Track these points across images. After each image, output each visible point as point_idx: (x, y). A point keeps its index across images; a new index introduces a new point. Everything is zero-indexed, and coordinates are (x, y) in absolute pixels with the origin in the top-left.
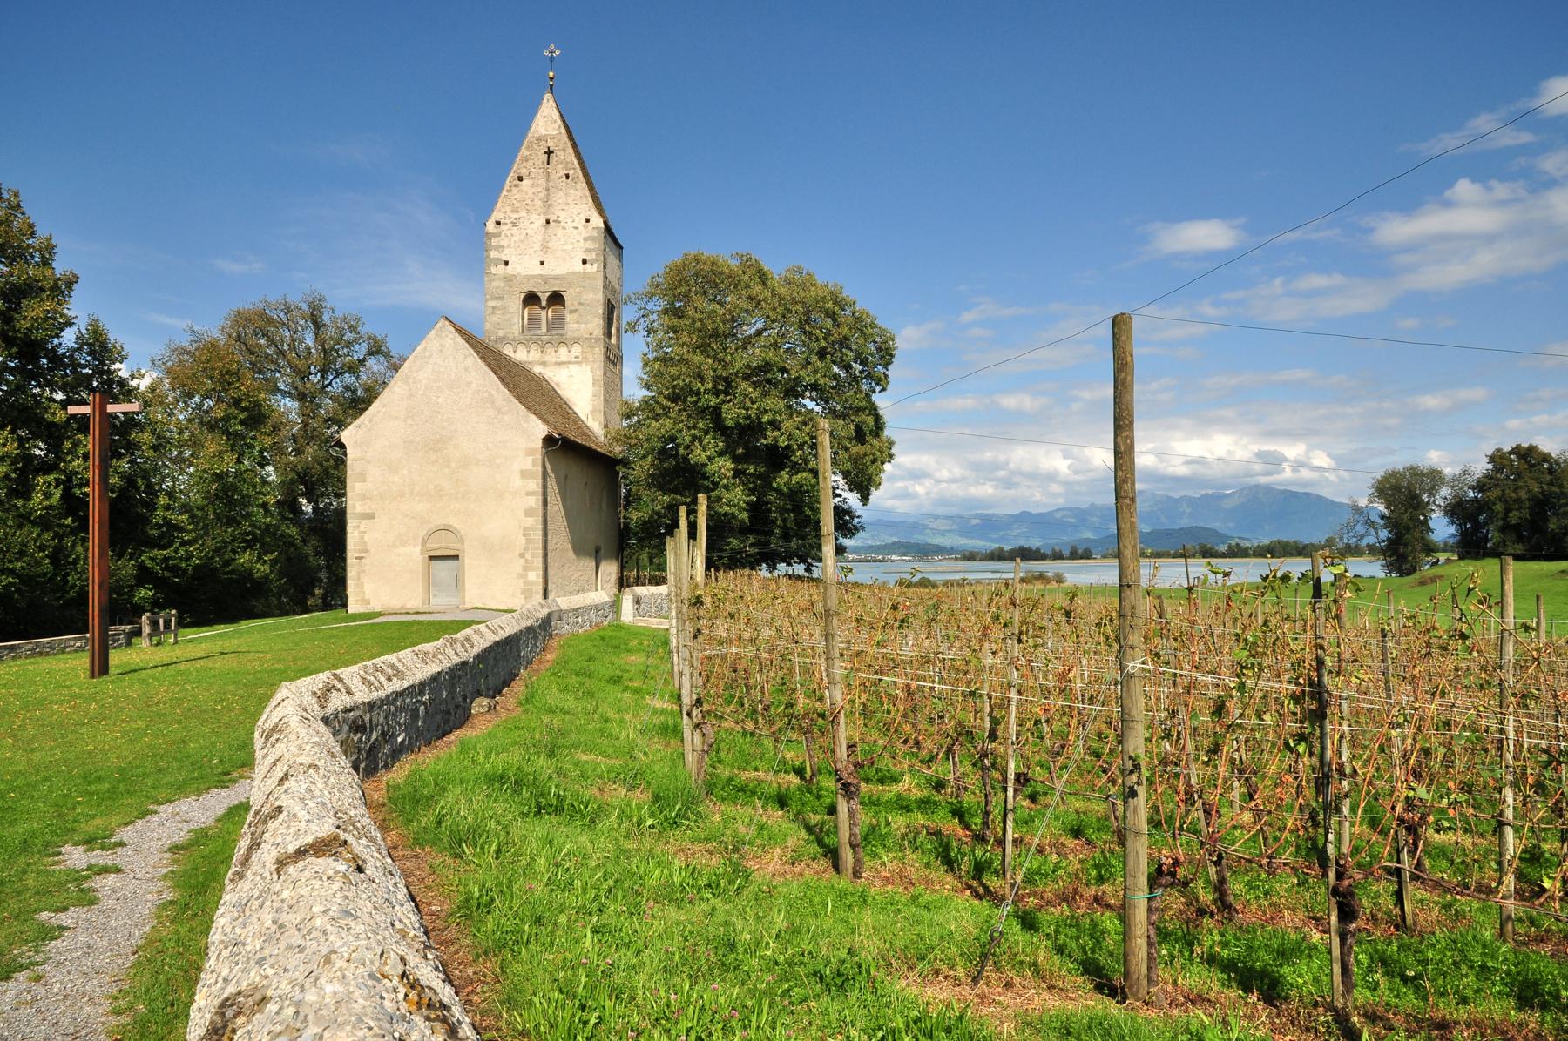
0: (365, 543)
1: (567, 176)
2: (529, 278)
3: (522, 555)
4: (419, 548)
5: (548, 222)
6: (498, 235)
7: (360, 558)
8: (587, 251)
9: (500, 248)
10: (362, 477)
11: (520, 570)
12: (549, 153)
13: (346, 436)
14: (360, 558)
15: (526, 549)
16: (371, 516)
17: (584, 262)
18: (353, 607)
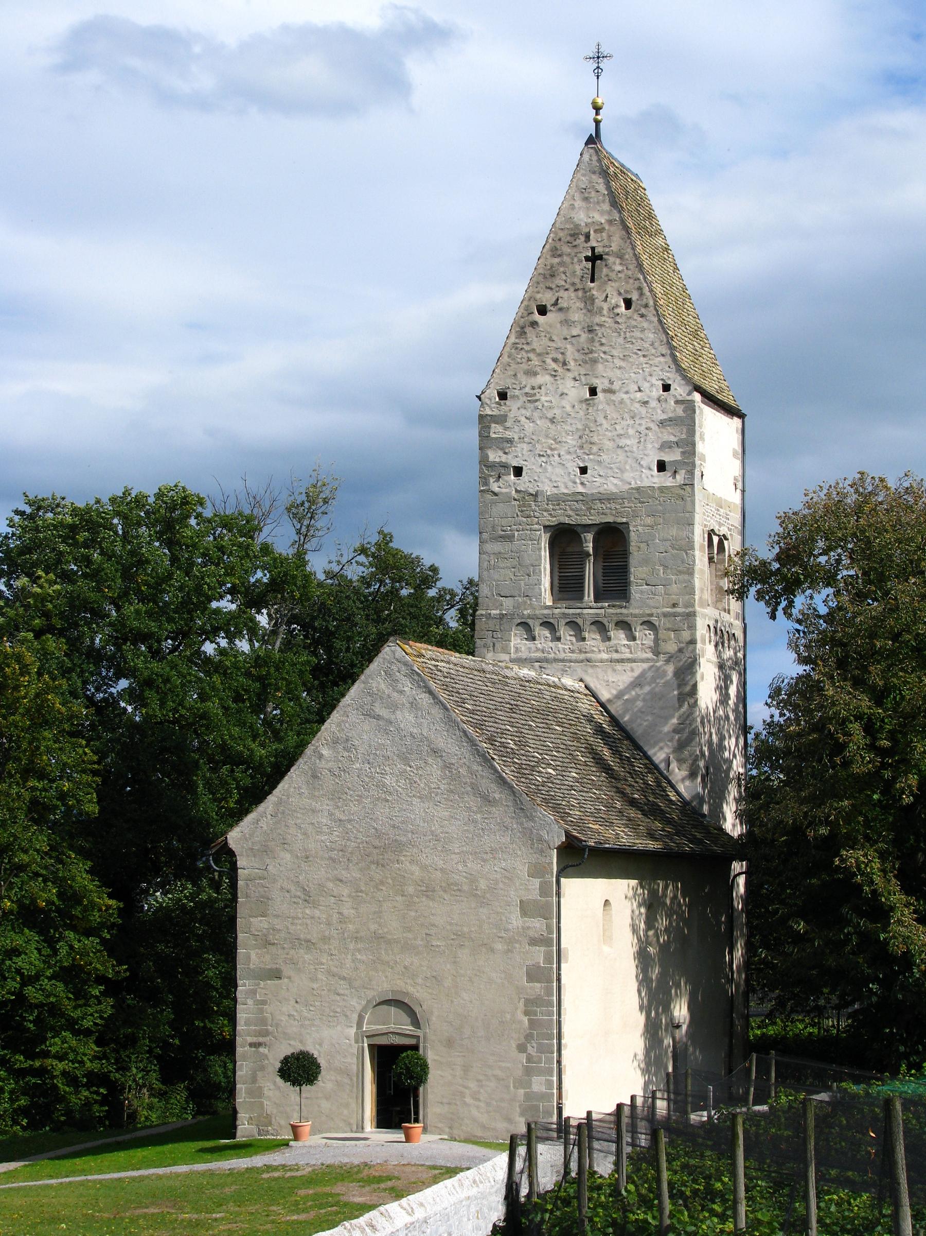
0: (263, 1021)
1: (628, 304)
2: (558, 500)
3: (522, 1048)
4: (354, 1030)
5: (593, 391)
6: (501, 420)
7: (260, 1045)
8: (665, 446)
9: (506, 443)
10: (263, 907)
11: (519, 1072)
12: (595, 258)
13: (235, 837)
14: (260, 1045)
15: (529, 1037)
16: (276, 975)
17: (661, 466)
18: (245, 1128)
